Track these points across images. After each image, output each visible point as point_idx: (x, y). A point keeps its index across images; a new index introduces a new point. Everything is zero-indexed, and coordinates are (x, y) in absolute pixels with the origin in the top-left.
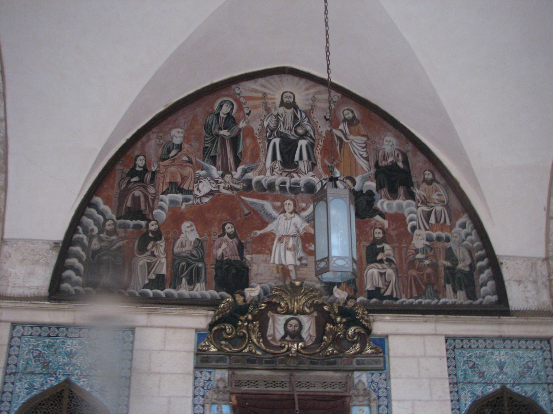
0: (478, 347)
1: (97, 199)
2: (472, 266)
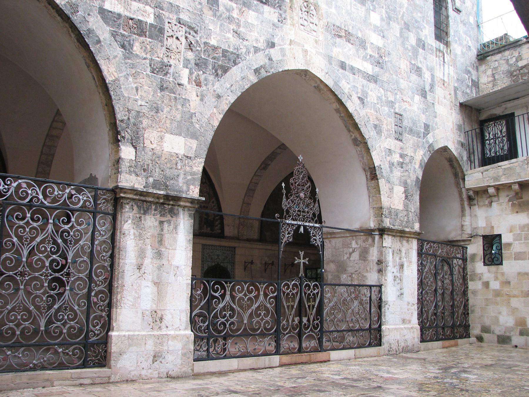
0: (212, 249)
2: (214, 219)
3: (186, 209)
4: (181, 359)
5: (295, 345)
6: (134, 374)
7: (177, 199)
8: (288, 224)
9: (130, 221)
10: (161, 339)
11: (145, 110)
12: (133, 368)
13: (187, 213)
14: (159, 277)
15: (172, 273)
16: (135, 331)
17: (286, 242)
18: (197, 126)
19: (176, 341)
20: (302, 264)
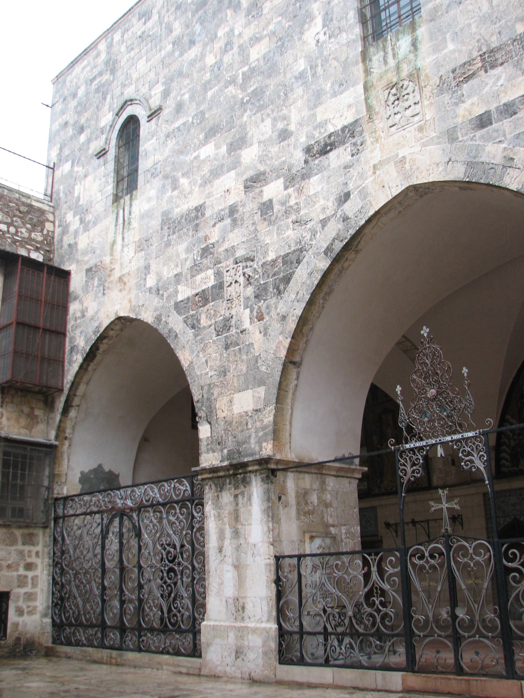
1: (508, 417)
3: (258, 473)
4: (263, 659)
5: (448, 657)
6: (219, 670)
7: (244, 465)
8: (412, 450)
9: (210, 503)
10: (241, 632)
11: (215, 380)
12: (219, 663)
13: (259, 478)
14: (238, 560)
15: (249, 553)
16: (221, 621)
17: (409, 480)
18: (263, 369)
19: (255, 635)
20: (445, 510)
